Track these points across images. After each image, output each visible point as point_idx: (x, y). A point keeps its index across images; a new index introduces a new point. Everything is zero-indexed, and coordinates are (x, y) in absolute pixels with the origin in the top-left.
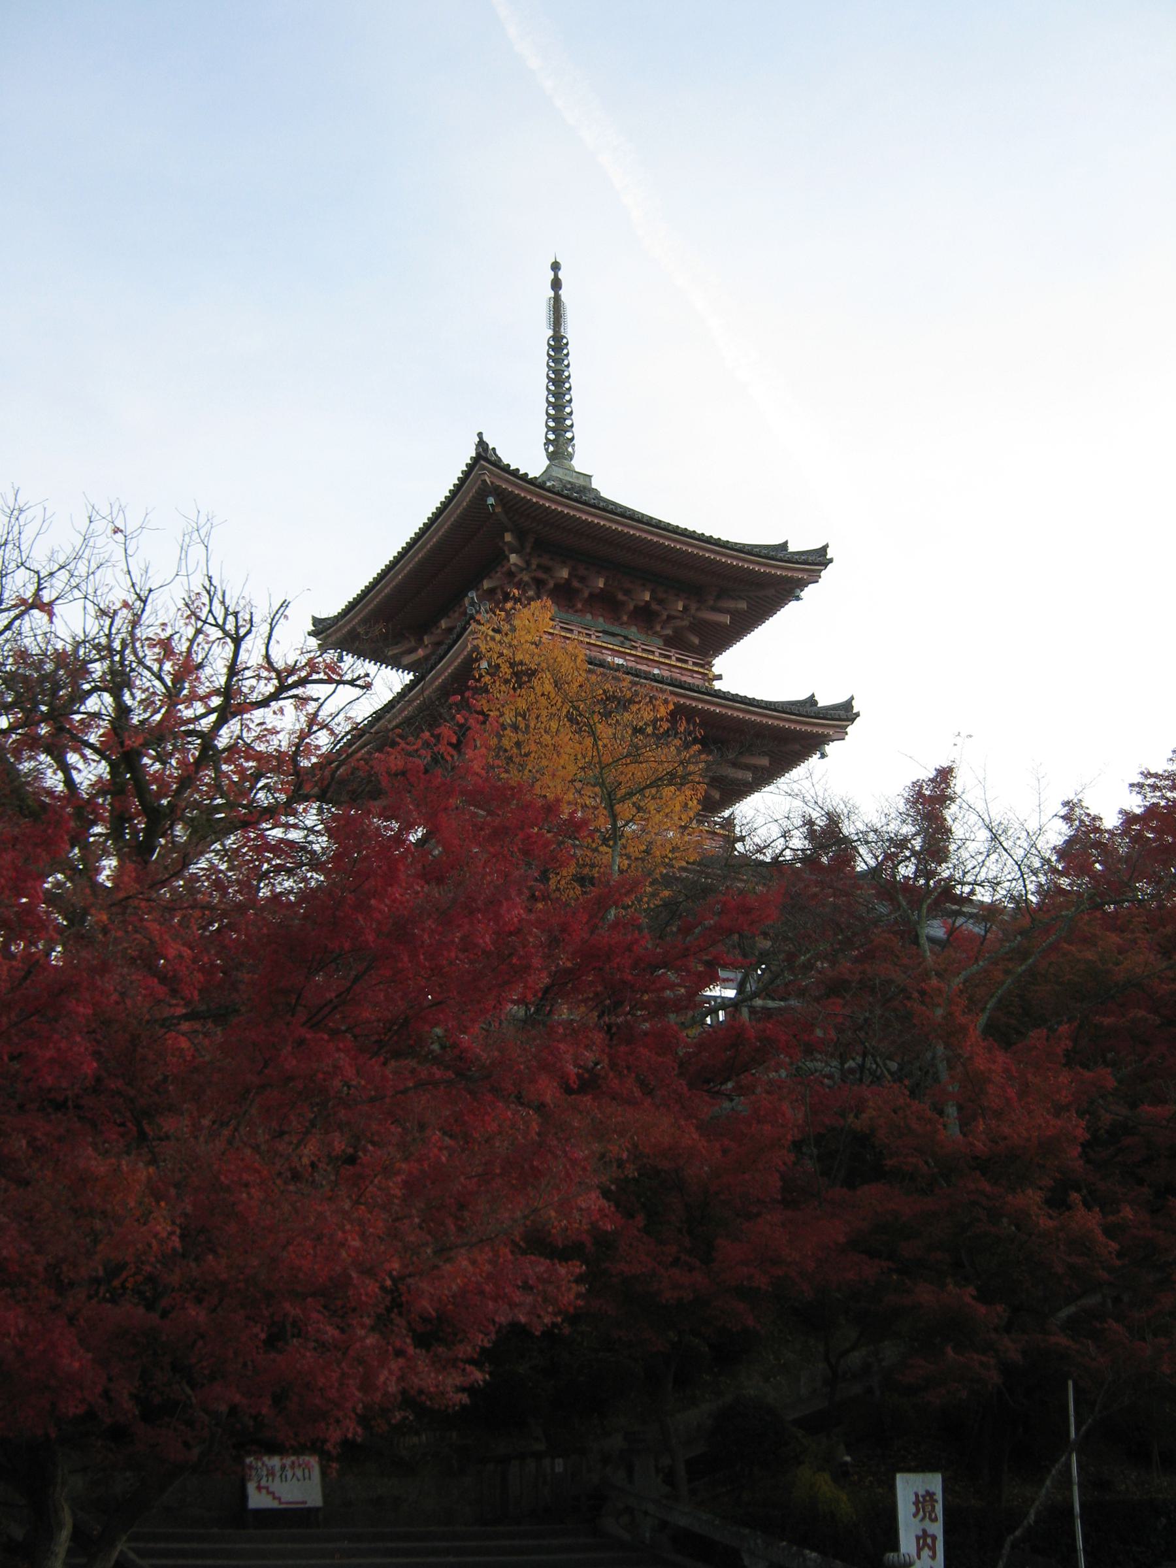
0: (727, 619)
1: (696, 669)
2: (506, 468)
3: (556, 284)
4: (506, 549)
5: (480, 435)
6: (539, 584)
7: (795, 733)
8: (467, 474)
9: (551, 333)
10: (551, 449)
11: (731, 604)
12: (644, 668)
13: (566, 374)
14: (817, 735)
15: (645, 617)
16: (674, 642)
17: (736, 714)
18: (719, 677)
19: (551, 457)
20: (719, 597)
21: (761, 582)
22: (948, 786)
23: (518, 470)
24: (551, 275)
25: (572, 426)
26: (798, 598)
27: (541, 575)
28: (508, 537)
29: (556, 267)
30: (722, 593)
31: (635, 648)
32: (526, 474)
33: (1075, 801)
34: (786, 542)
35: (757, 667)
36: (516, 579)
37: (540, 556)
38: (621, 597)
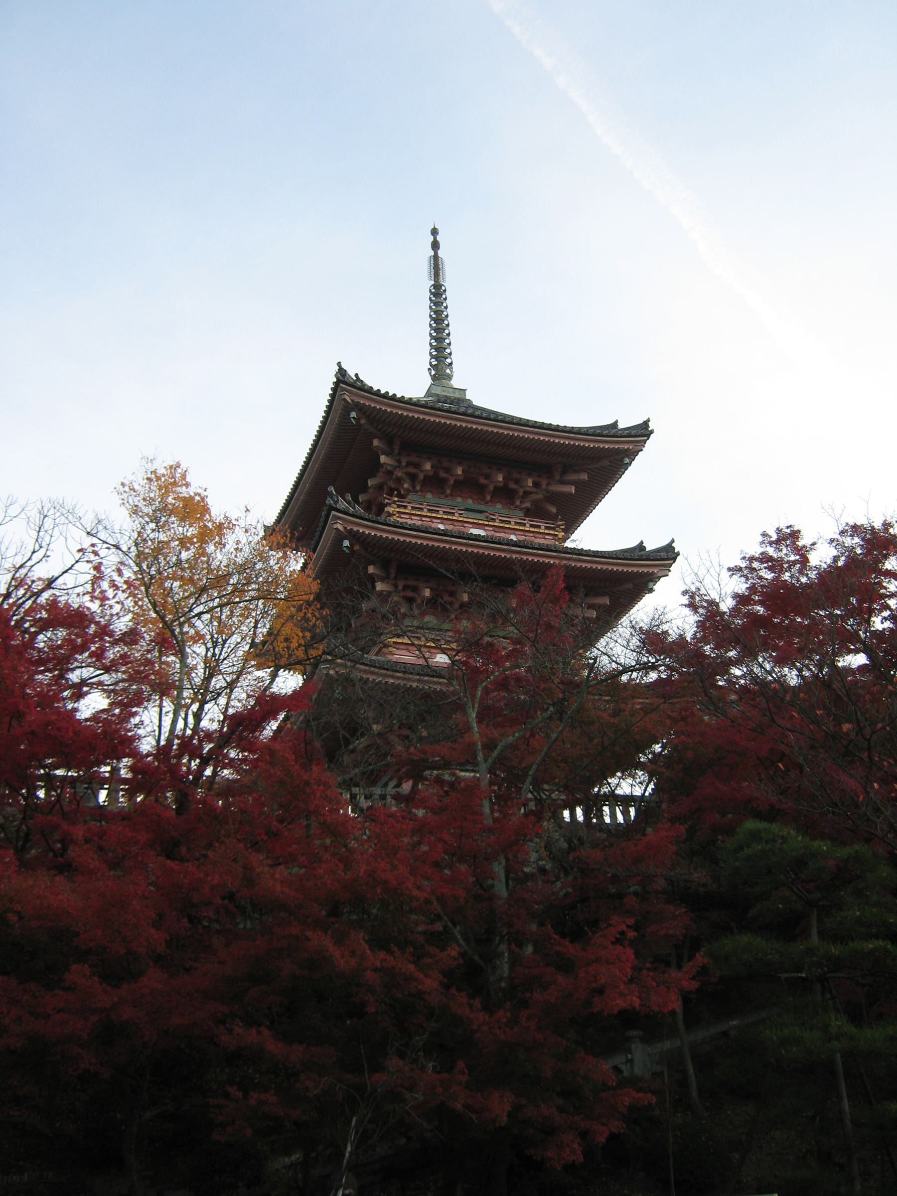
1: (547, 531)
2: (370, 390)
3: (435, 245)
5: (339, 364)
10: (433, 372)
12: (502, 535)
14: (642, 575)
15: (505, 495)
16: (536, 512)
19: (434, 378)
20: (564, 472)
27: (412, 470)
29: (434, 232)
30: (567, 469)
31: (494, 520)
32: (379, 390)
33: (694, 590)
34: (617, 422)
38: (482, 481)
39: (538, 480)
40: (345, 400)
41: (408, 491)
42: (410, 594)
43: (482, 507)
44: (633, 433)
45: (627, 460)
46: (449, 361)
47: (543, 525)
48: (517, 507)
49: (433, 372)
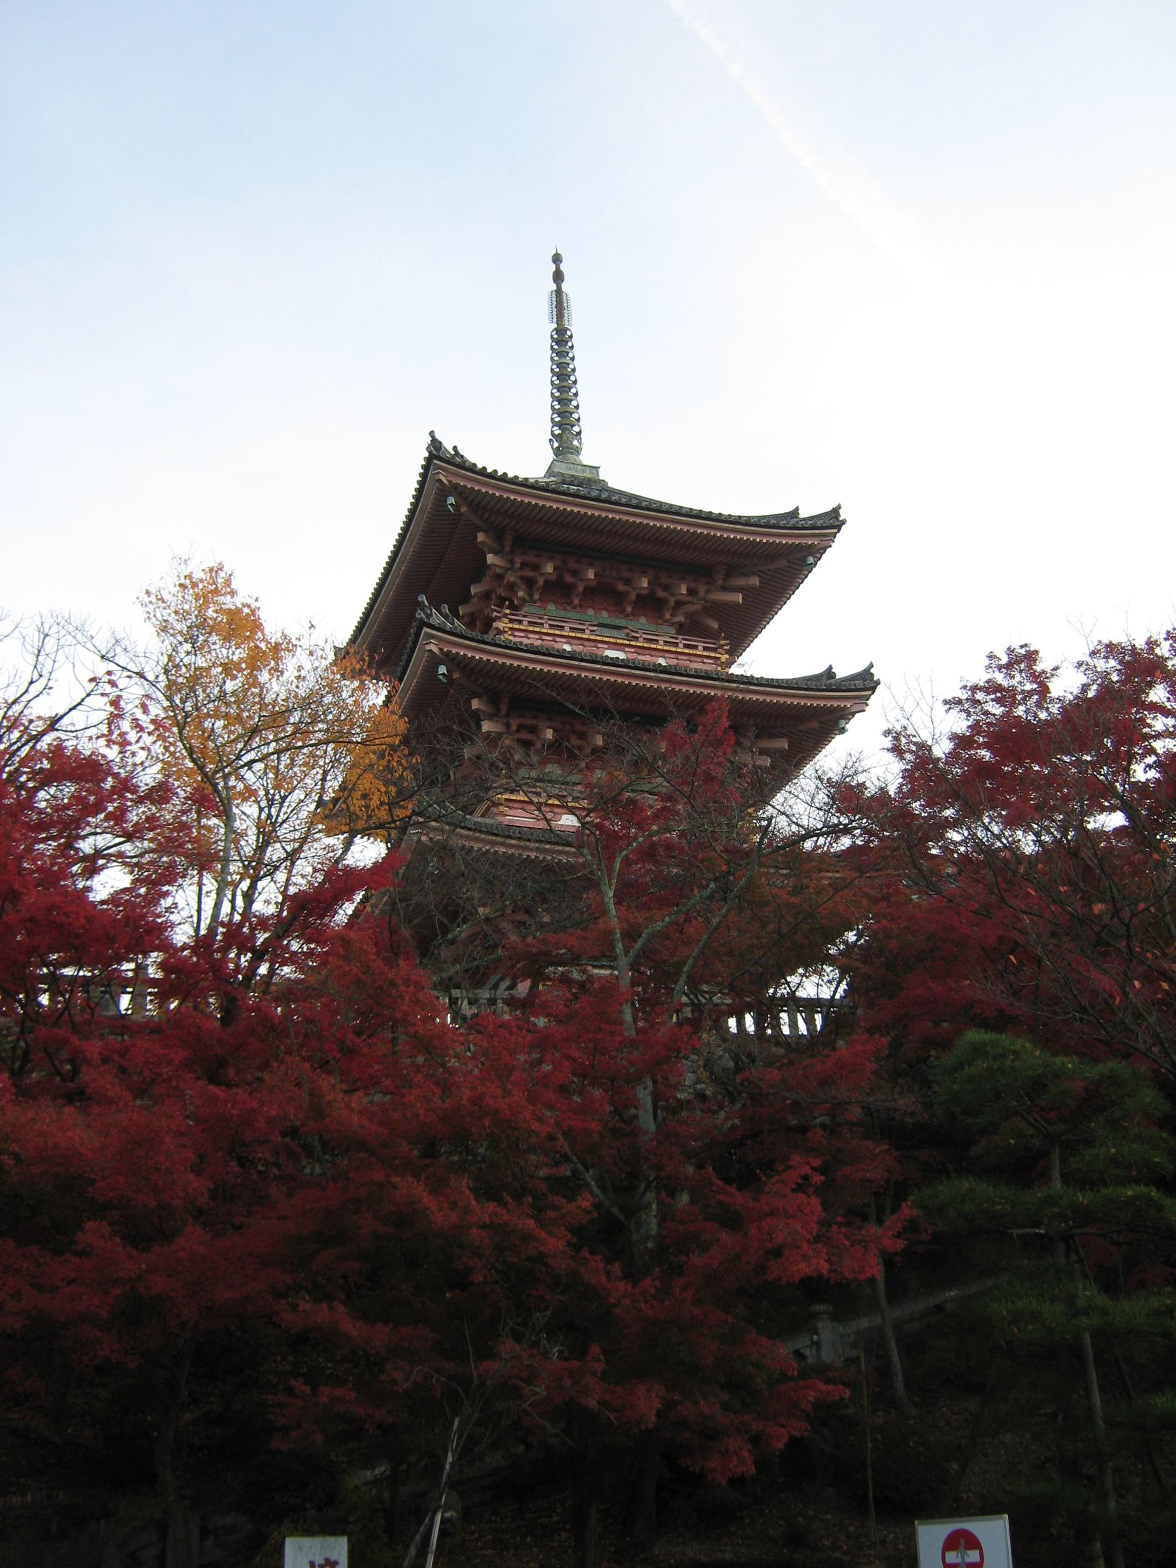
2: (472, 468)
3: (558, 277)
5: (432, 434)
7: (815, 710)
10: (556, 445)
11: (742, 582)
12: (648, 658)
14: (832, 710)
15: (651, 605)
16: (691, 628)
17: (755, 698)
19: (557, 452)
20: (728, 576)
24: (553, 267)
27: (528, 573)
28: (481, 537)
29: (557, 259)
34: (797, 509)
37: (524, 554)
38: (621, 587)
39: (694, 585)
40: (440, 481)
41: (524, 601)
42: (529, 737)
44: (819, 523)
45: (811, 560)
46: (576, 429)
47: (701, 646)
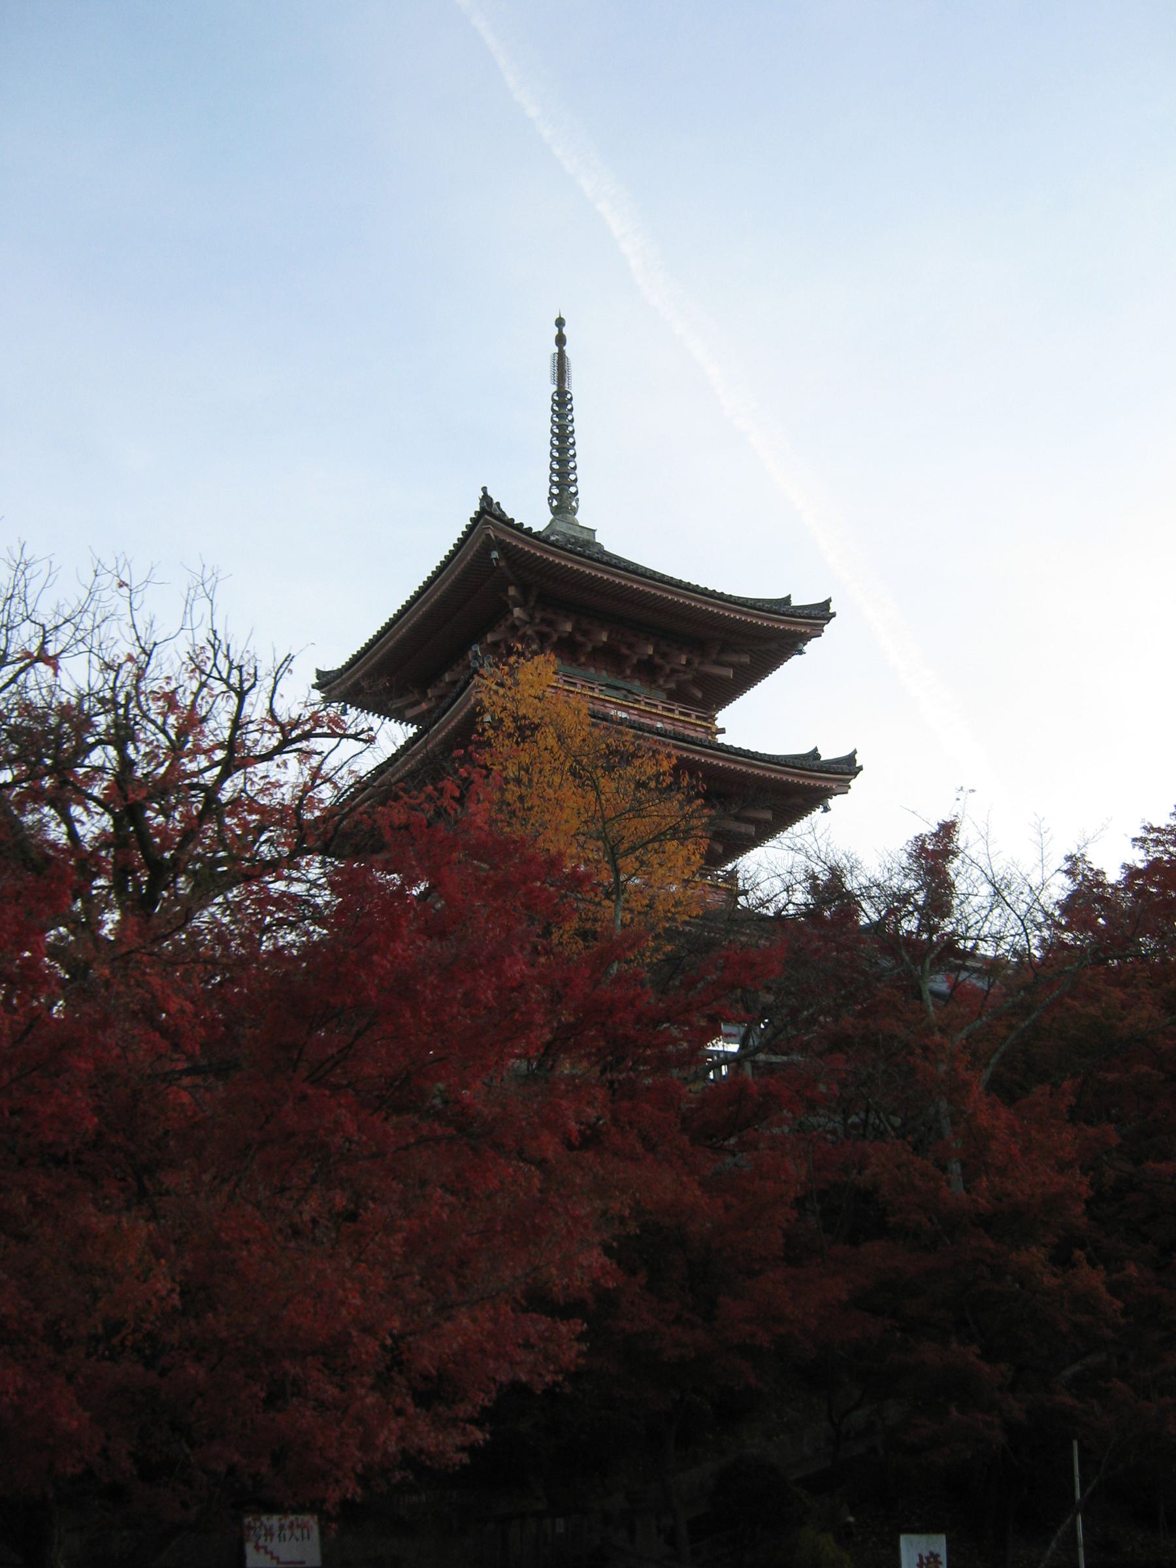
0: (730, 673)
1: (699, 722)
2: (510, 523)
3: (561, 340)
4: (510, 602)
5: (484, 489)
6: (543, 638)
8: (471, 529)
9: (555, 388)
10: (555, 503)
11: (734, 658)
13: (570, 429)
15: (648, 671)
16: (678, 695)
17: (739, 767)
18: (723, 731)
19: (555, 511)
21: (765, 635)
22: (951, 841)
23: (522, 524)
24: (556, 331)
25: (576, 480)
26: (801, 652)
27: (545, 629)
28: (512, 591)
29: (560, 323)
31: (638, 701)
32: (530, 529)
35: (761, 721)
36: (520, 633)
40: (488, 535)
43: (620, 684)
44: (814, 613)
47: (694, 714)
48: (659, 687)
49: (555, 503)
